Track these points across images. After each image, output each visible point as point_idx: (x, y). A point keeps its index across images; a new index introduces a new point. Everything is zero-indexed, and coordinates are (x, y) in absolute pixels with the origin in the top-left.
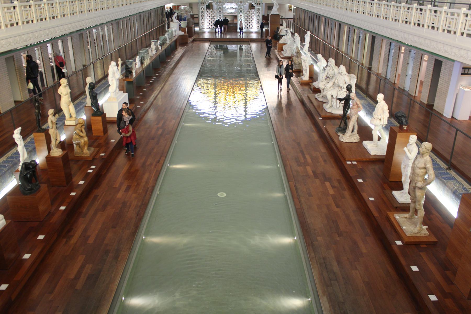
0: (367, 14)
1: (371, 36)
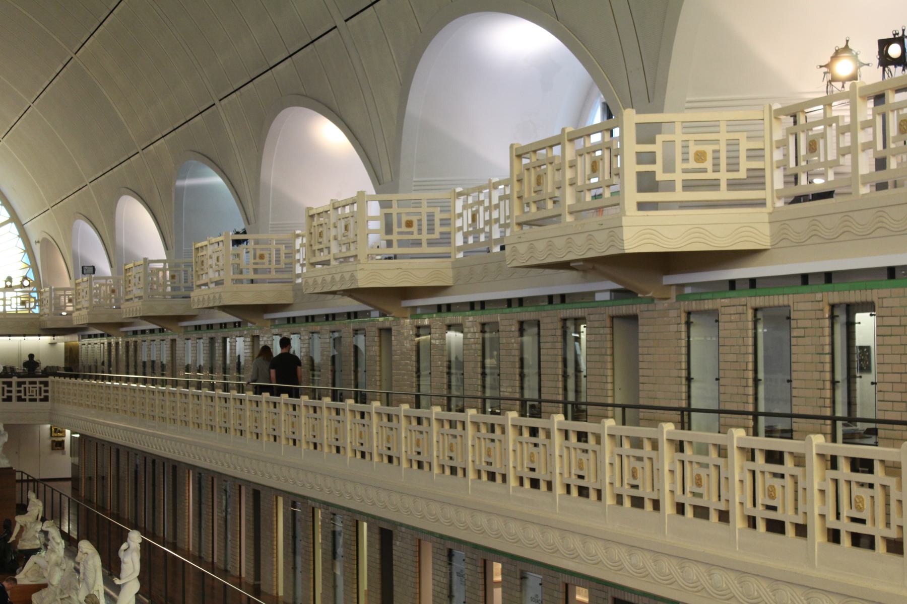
0: (350, 454)
1: (377, 531)
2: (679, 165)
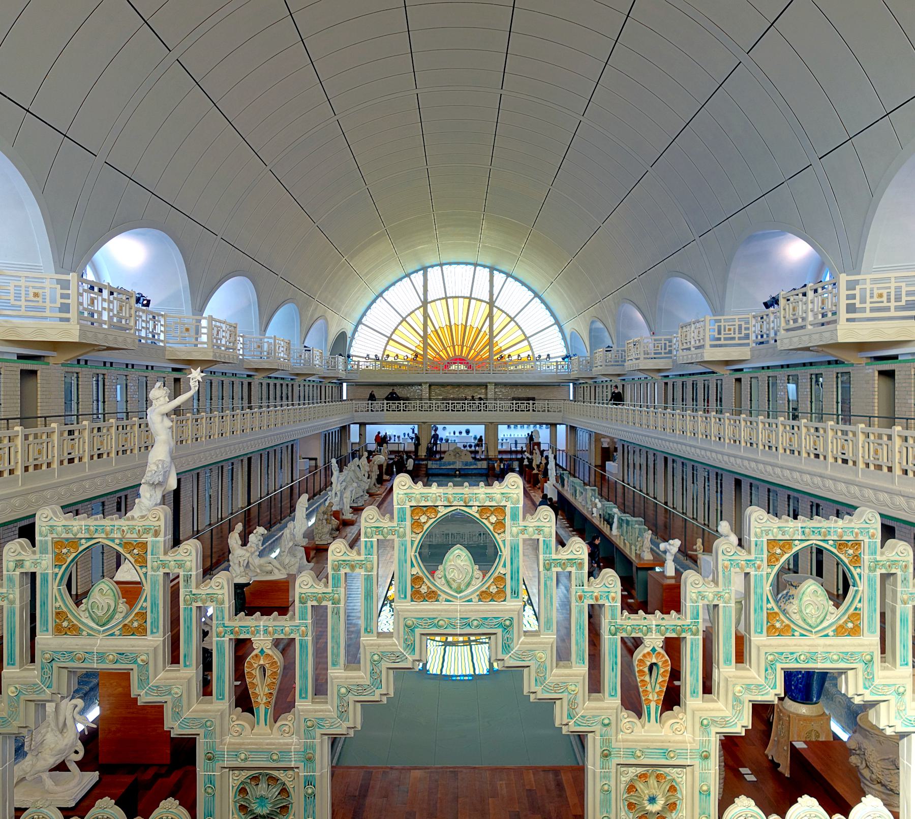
2: (868, 300)
